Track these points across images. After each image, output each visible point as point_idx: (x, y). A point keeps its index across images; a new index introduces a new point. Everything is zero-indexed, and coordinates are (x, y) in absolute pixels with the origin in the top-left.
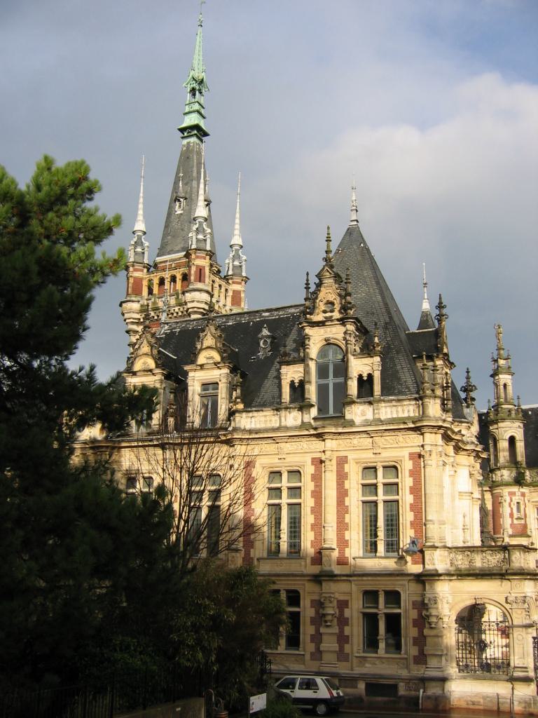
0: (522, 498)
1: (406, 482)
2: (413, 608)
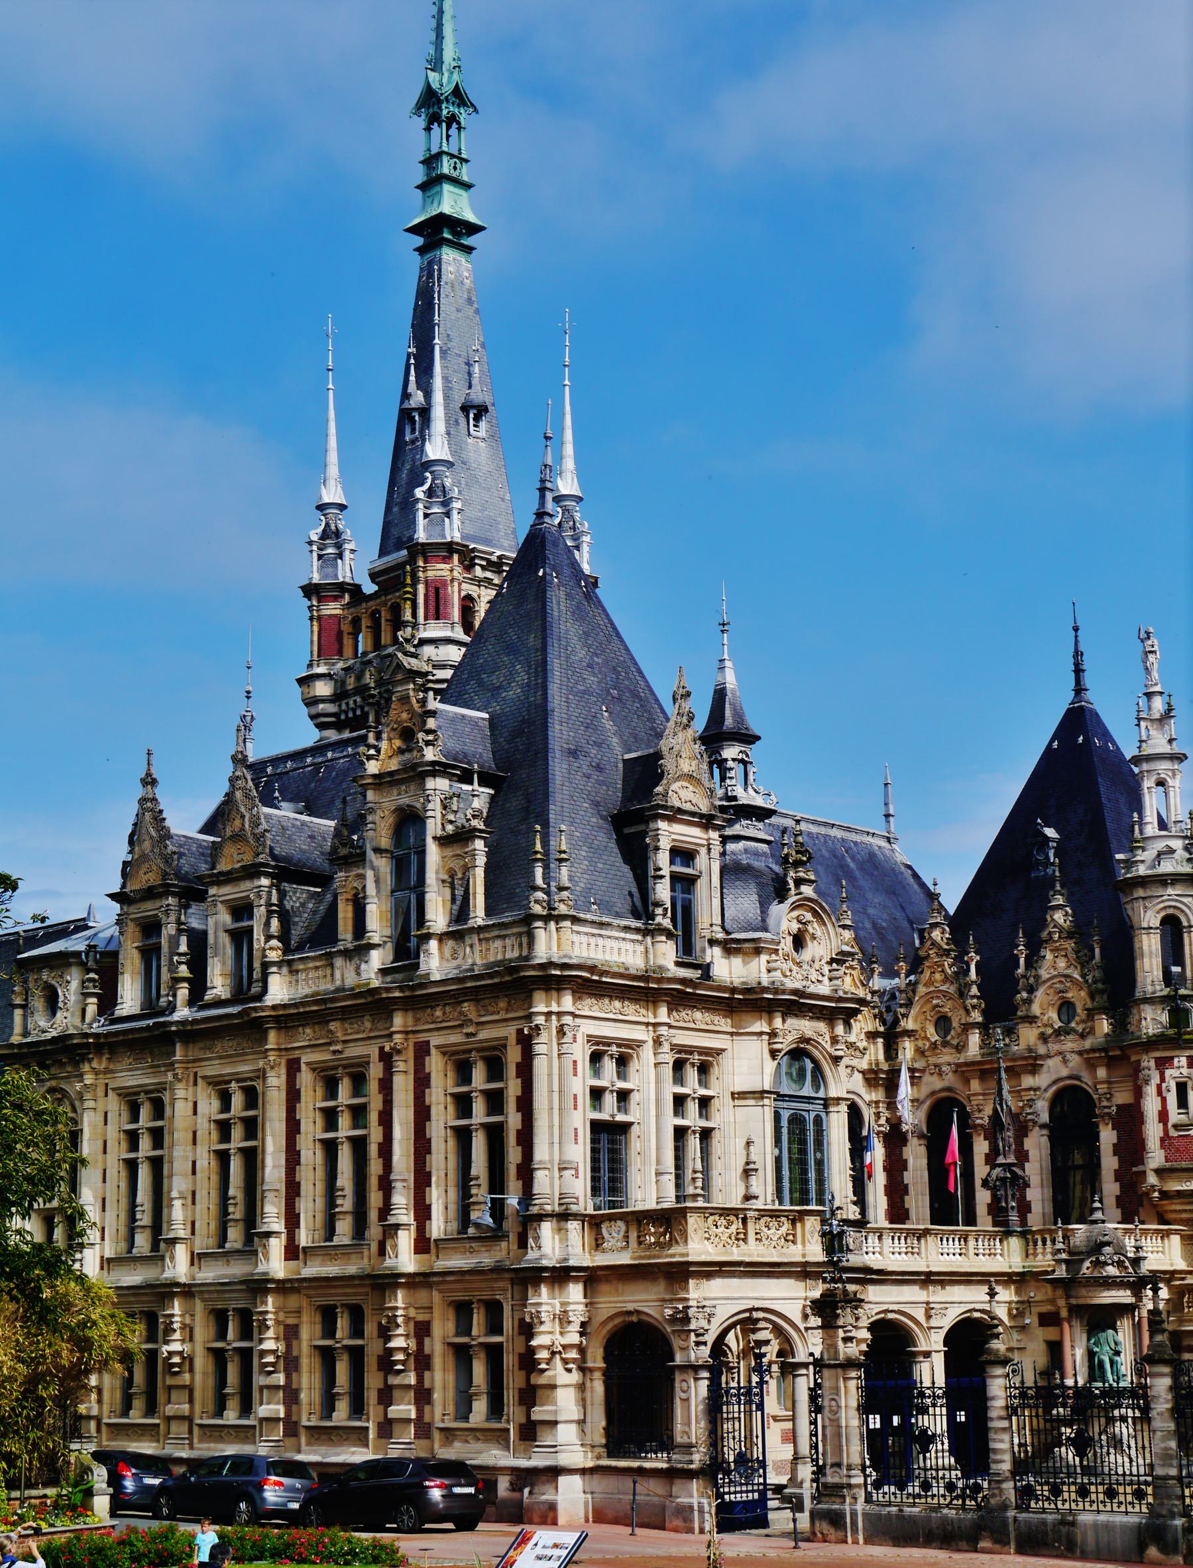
1: (513, 1088)
2: (520, 1334)
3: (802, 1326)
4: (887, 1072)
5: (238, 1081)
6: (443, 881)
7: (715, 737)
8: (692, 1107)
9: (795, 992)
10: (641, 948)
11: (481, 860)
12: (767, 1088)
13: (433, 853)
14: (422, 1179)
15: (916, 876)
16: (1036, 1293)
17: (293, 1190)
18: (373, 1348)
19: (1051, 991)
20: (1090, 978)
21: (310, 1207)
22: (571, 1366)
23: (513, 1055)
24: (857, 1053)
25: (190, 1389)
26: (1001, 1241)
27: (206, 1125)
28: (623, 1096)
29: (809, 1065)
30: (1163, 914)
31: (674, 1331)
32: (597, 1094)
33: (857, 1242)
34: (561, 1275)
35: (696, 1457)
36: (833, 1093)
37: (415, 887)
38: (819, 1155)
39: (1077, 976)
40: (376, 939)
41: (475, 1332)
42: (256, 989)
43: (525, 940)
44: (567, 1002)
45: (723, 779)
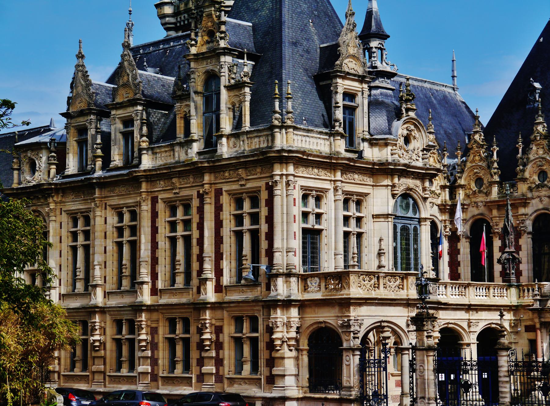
1: (264, 212)
2: (267, 332)
3: (406, 330)
4: (450, 206)
5: (127, 207)
6: (229, 108)
7: (366, 37)
8: (353, 222)
9: (405, 165)
10: (328, 143)
11: (248, 98)
12: (390, 213)
13: (224, 94)
14: (219, 256)
15: (467, 107)
16: (525, 316)
17: (154, 261)
18: (194, 339)
21: (163, 269)
22: (292, 348)
23: (264, 195)
24: (436, 196)
25: (104, 358)
26: (506, 290)
27: (111, 229)
28: (318, 216)
29: (411, 202)
31: (343, 332)
32: (305, 215)
33: (434, 289)
34: (287, 304)
35: (353, 393)
36: (423, 216)
37: (215, 111)
38: (415, 246)
40: (196, 137)
41: (244, 331)
42: (135, 162)
43: (270, 138)
44: (291, 169)
45: (370, 57)
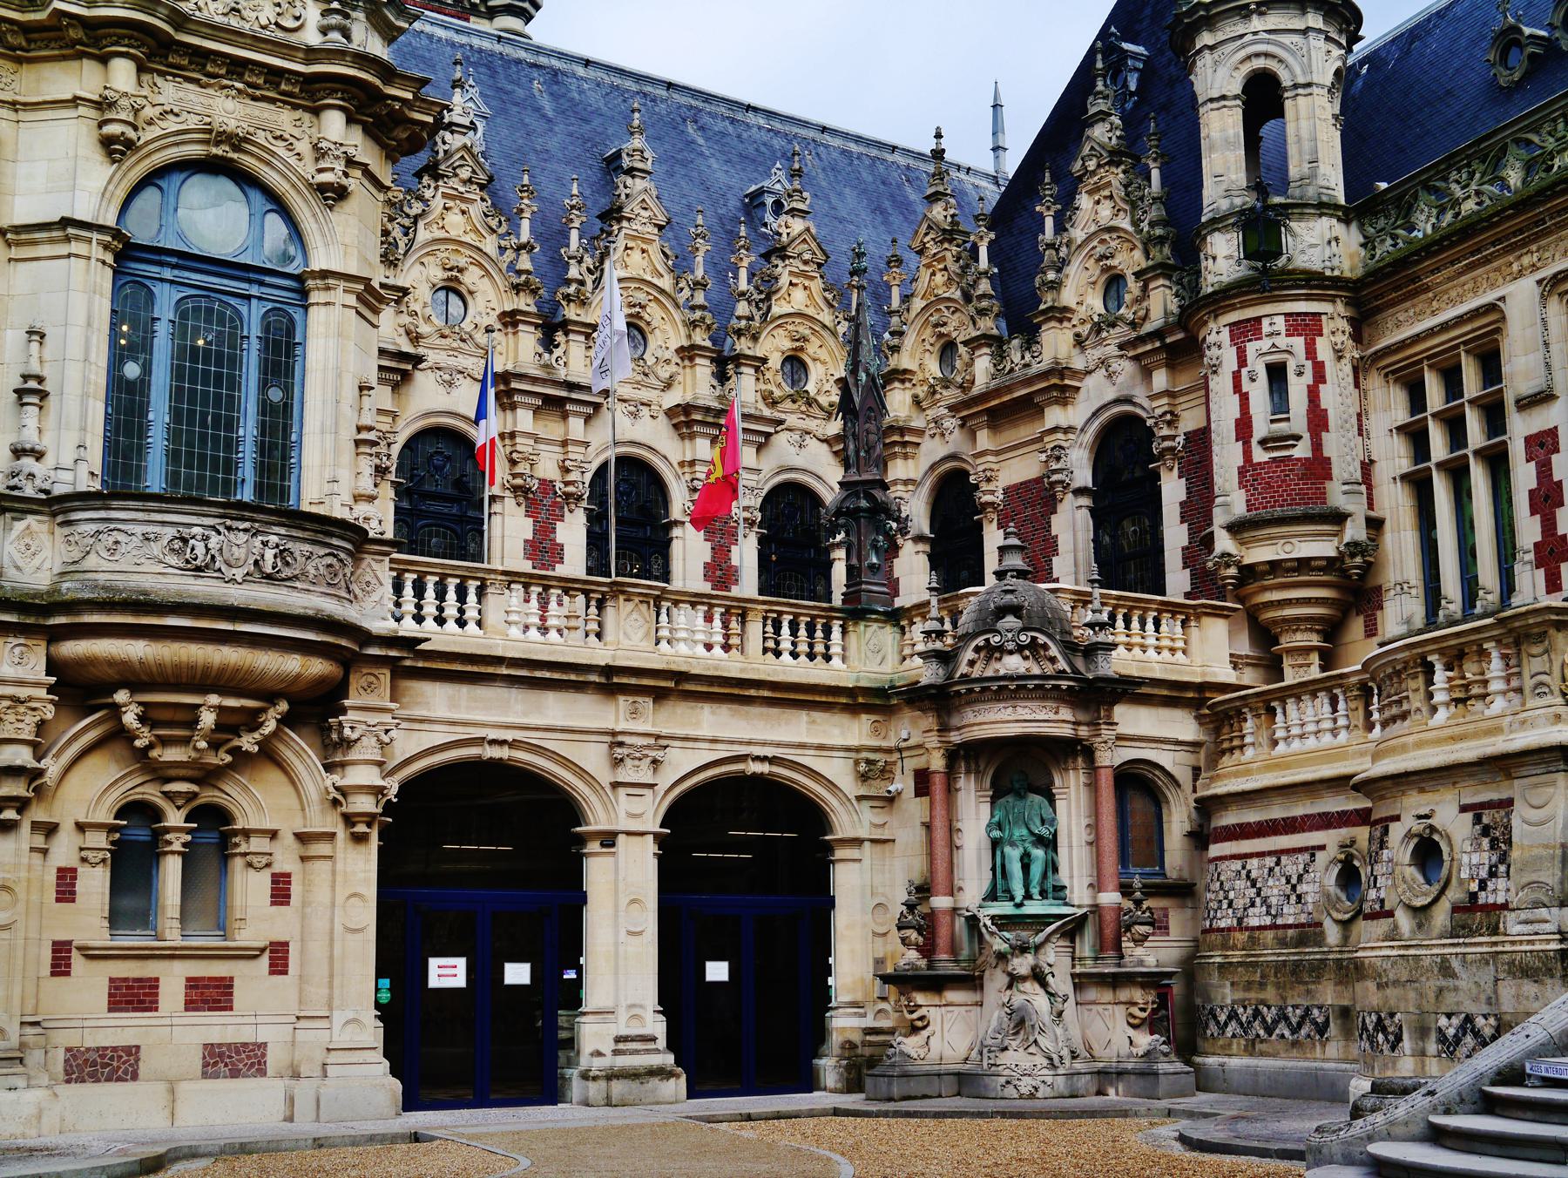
0: (1298, 343)
16: (912, 728)
19: (1092, 260)
20: (1145, 226)
30: (1246, 68)
36: (318, 262)
39: (1125, 223)
